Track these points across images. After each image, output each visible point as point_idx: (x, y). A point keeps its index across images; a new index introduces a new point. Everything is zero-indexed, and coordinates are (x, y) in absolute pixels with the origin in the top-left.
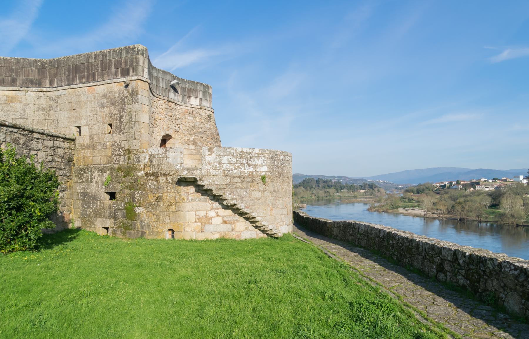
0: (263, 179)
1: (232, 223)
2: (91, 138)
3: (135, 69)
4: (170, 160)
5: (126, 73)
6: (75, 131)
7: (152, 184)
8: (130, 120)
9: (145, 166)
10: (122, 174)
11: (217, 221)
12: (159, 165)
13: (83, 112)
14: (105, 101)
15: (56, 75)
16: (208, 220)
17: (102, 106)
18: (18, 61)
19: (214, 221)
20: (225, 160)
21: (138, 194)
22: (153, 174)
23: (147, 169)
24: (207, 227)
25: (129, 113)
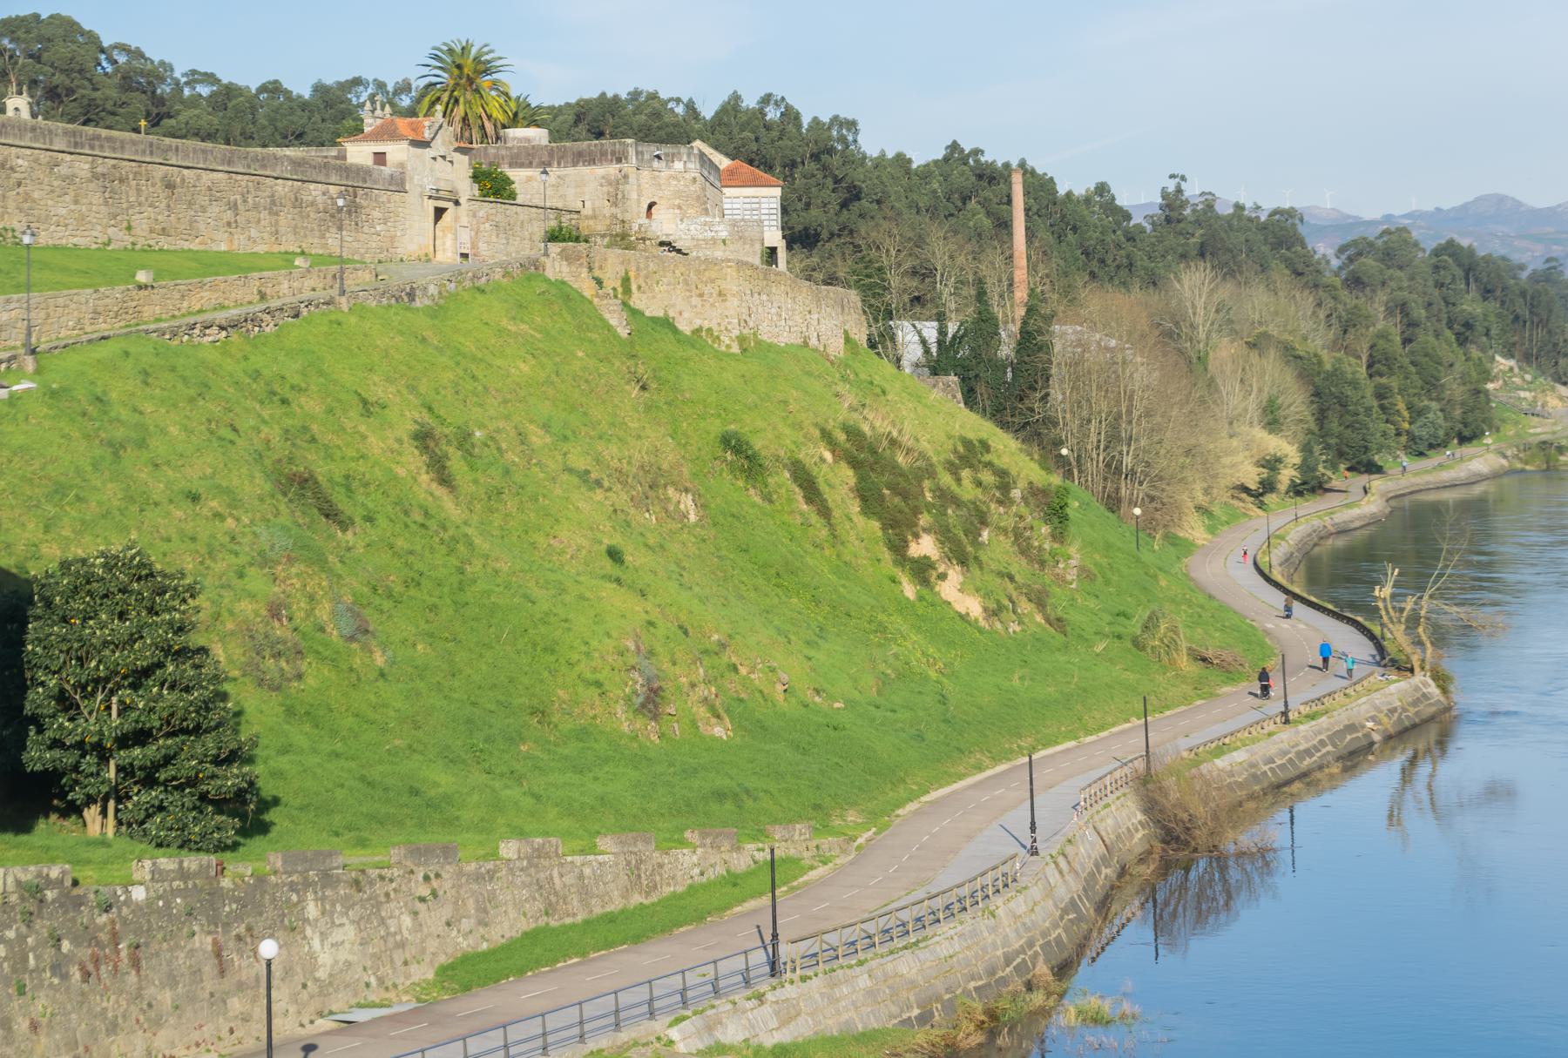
0: (724, 241)
5: (619, 160)
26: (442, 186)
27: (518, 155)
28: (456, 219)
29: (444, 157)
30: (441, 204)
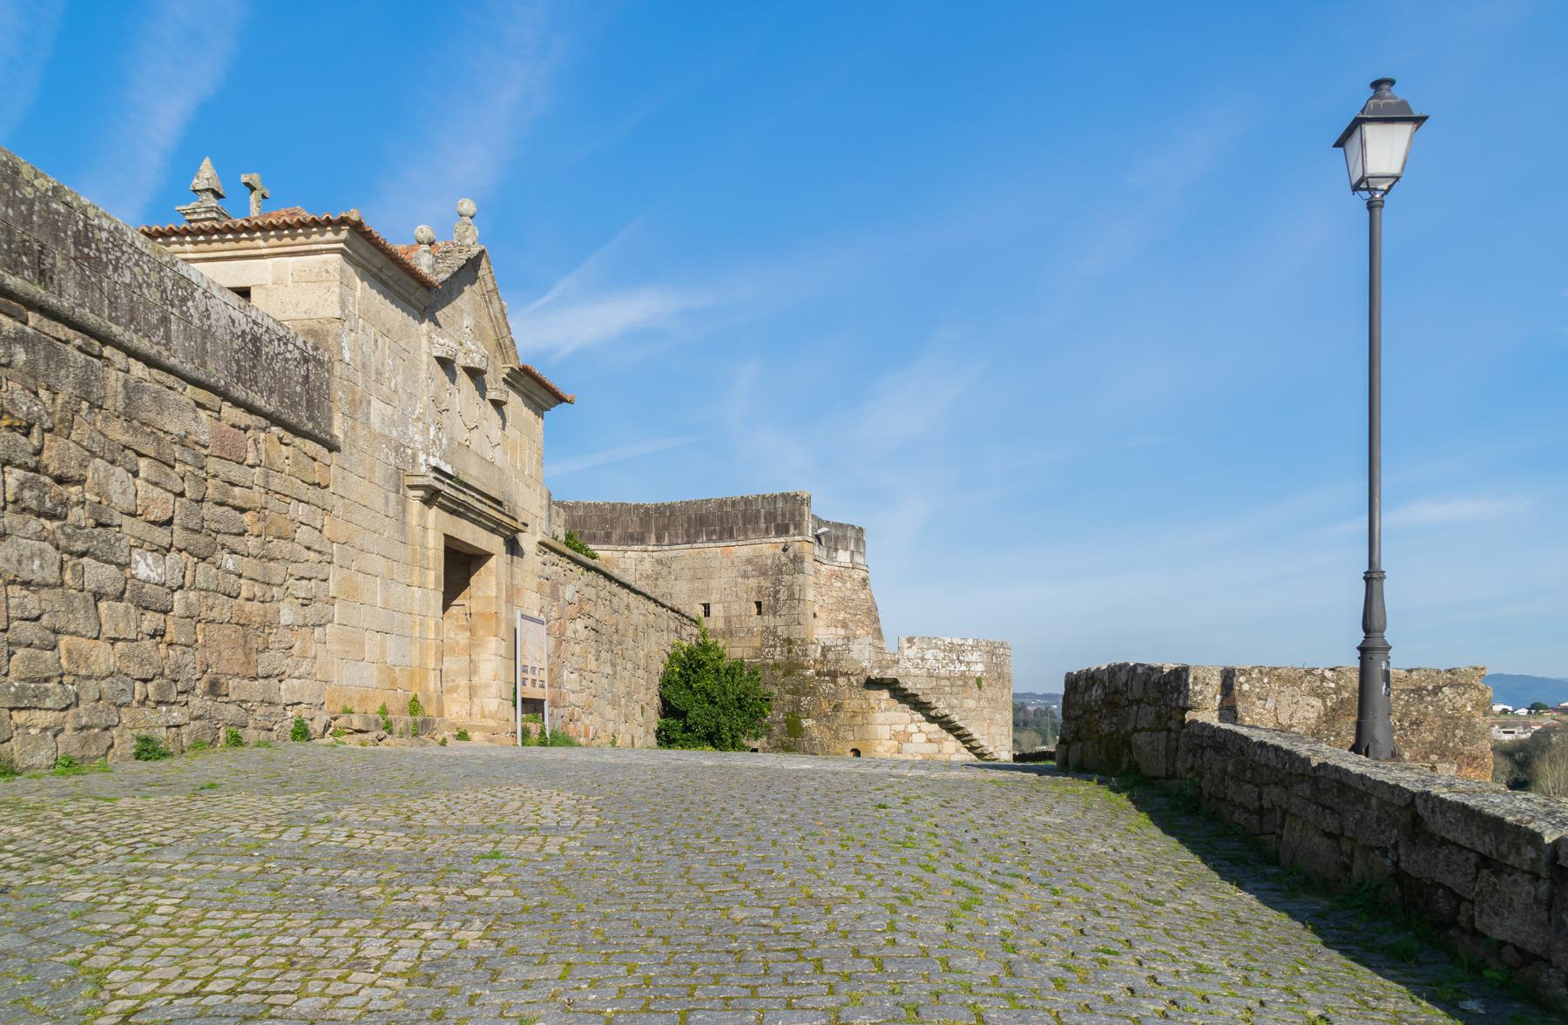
0: (979, 681)
1: (939, 742)
2: (728, 620)
3: (799, 526)
4: (854, 655)
5: (782, 530)
6: (700, 610)
7: (827, 687)
8: (791, 596)
9: (815, 661)
10: (779, 673)
11: (919, 738)
12: (837, 661)
13: (714, 583)
14: (750, 568)
15: (666, 528)
16: (908, 737)
17: (745, 576)
18: (613, 506)
19: (915, 738)
20: (929, 655)
21: (805, 701)
22: (828, 674)
23: (818, 666)
24: (906, 746)
25: (790, 587)
26: (473, 474)
27: (584, 521)
28: (512, 594)
29: (475, 374)
30: (471, 535)
